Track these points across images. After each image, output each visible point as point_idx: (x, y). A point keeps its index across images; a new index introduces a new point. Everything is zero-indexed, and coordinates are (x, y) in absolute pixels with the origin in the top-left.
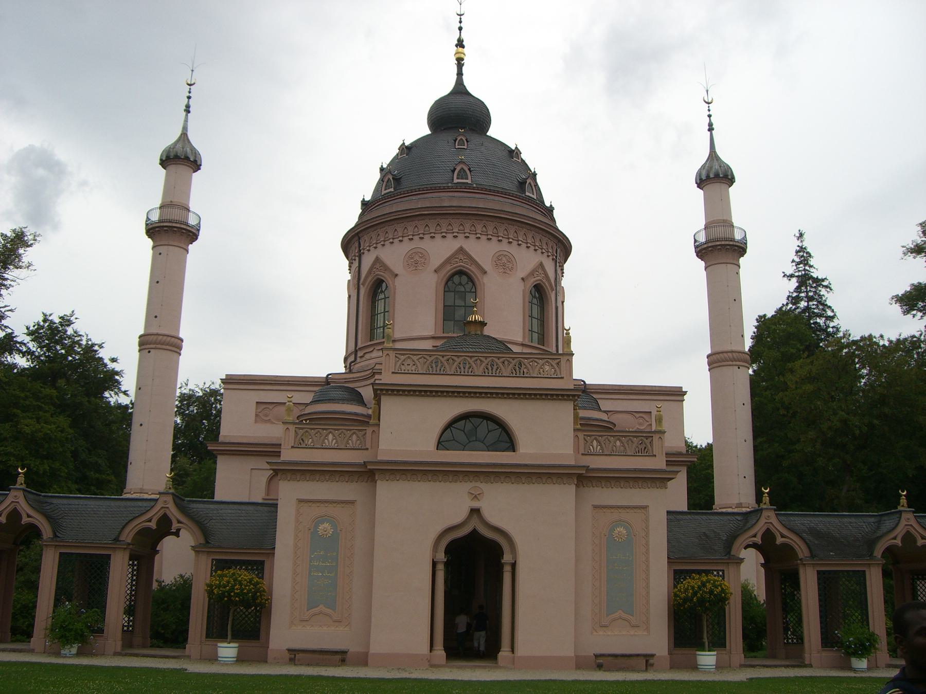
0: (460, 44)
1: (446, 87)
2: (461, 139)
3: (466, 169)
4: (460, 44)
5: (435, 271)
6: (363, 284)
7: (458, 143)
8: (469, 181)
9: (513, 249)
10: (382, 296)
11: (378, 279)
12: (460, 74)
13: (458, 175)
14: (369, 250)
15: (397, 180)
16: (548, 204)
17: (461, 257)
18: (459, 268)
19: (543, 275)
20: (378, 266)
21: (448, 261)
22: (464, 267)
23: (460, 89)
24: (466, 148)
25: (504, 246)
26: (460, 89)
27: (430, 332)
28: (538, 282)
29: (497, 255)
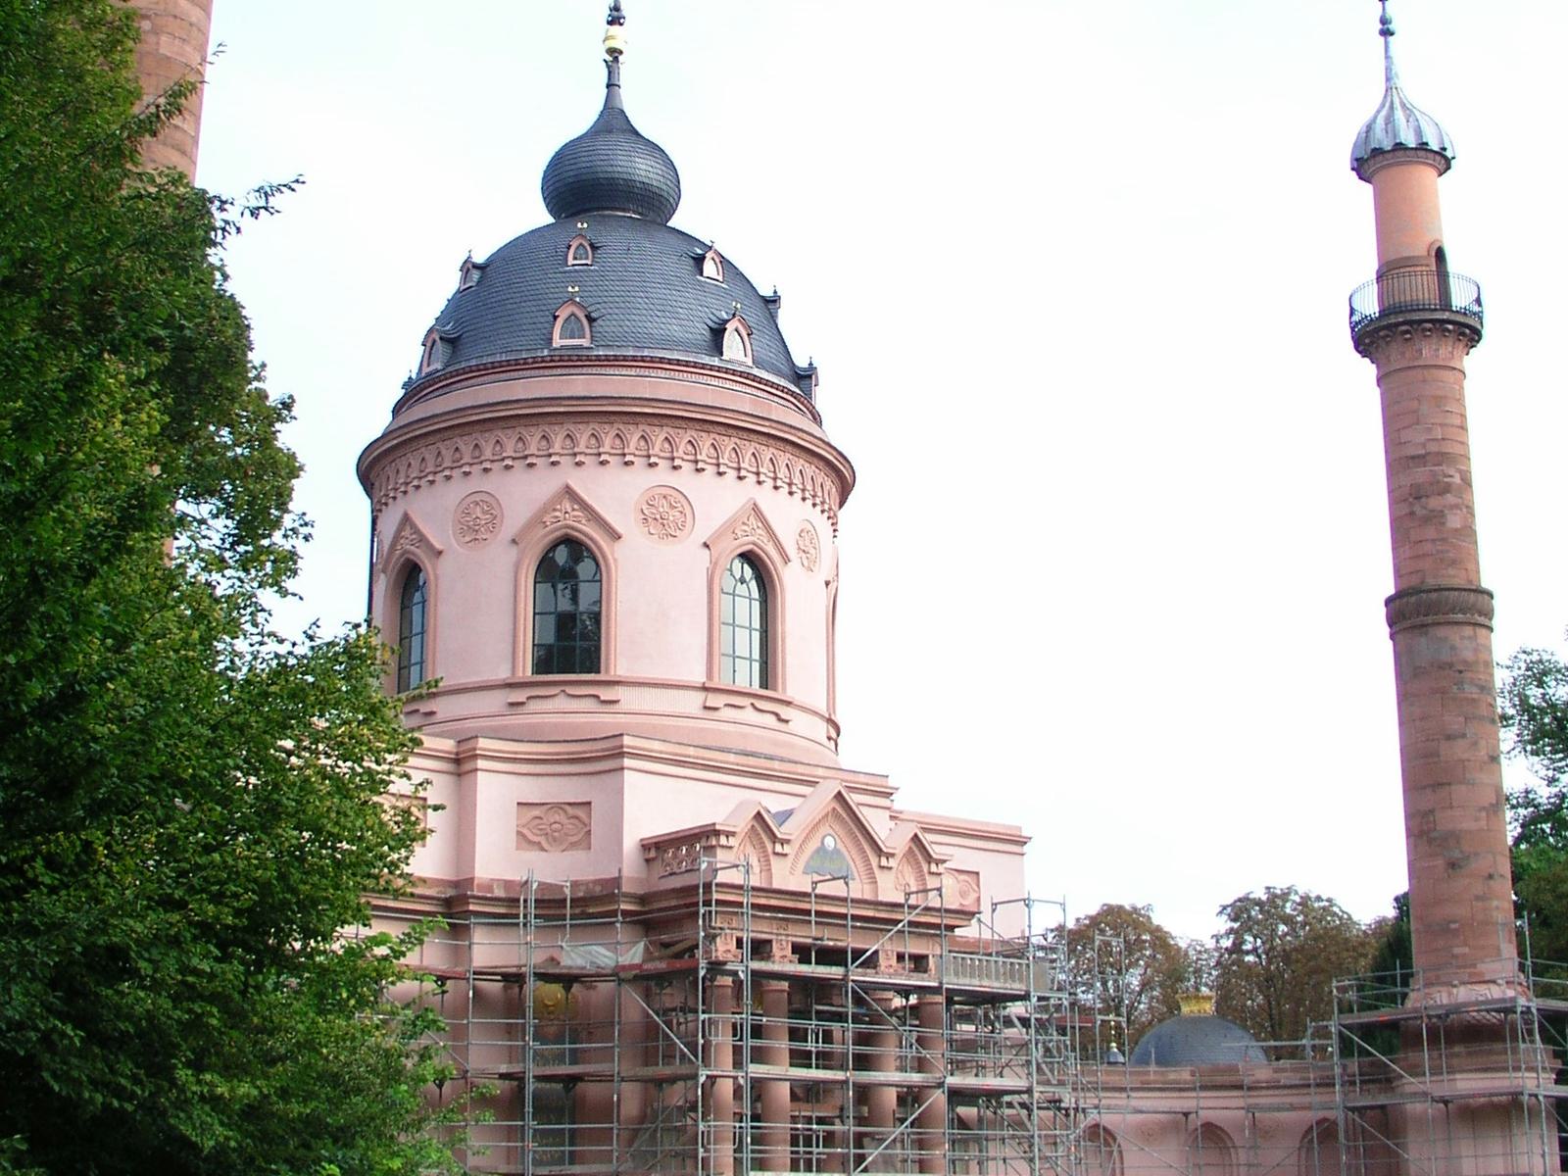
0: (615, 19)
1: (580, 117)
2: (581, 244)
4: (615, 19)
5: (514, 541)
6: (384, 571)
7: (575, 253)
10: (417, 597)
11: (408, 560)
14: (394, 498)
15: (452, 342)
18: (564, 531)
19: (759, 531)
20: (407, 532)
21: (537, 520)
22: (573, 528)
23: (613, 121)
24: (589, 262)
25: (662, 475)
26: (613, 121)
27: (503, 674)
28: (750, 547)
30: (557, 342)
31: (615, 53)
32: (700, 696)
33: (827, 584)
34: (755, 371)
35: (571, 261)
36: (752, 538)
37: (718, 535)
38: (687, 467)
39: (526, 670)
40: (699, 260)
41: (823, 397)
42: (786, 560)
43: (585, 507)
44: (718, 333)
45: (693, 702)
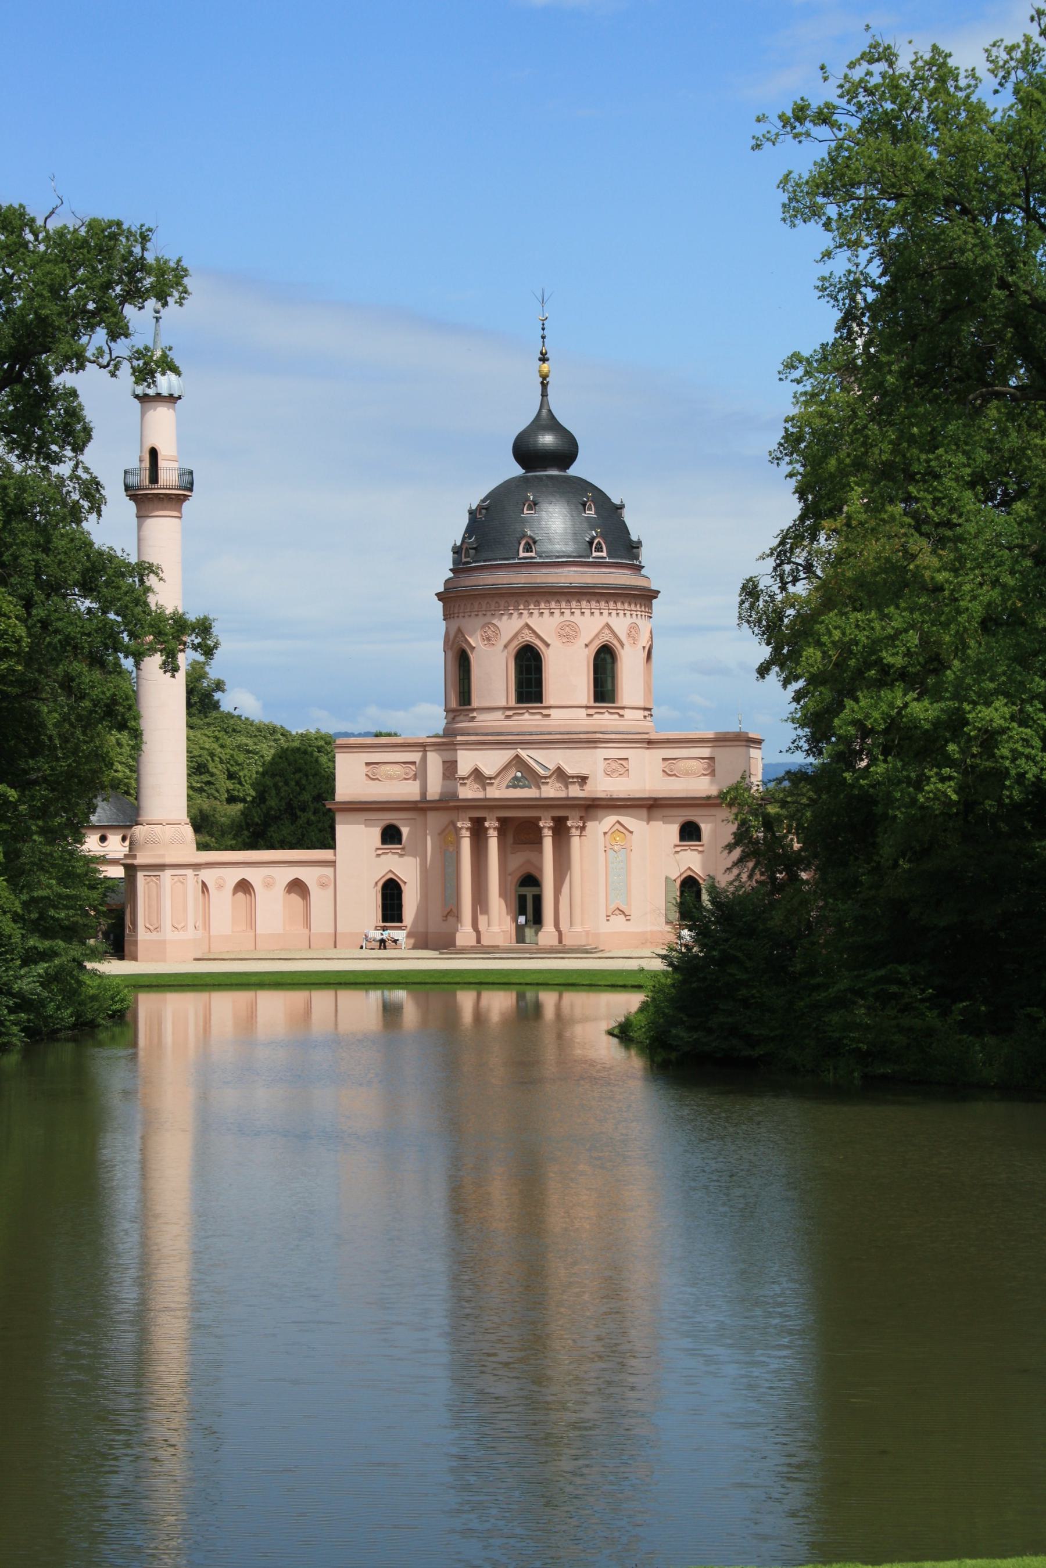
3: (531, 542)
4: (544, 359)
8: (533, 554)
9: (577, 618)
12: (544, 394)
13: (524, 548)
16: (634, 537)
17: (527, 631)
20: (460, 635)
27: (503, 704)
29: (562, 625)
30: (522, 554)
31: (544, 377)
32: (584, 712)
33: (644, 647)
34: (607, 560)
35: (525, 512)
36: (606, 637)
37: (591, 642)
38: (577, 612)
39: (512, 703)
40: (584, 505)
41: (646, 556)
42: (622, 645)
43: (534, 632)
44: (591, 543)
45: (583, 713)
